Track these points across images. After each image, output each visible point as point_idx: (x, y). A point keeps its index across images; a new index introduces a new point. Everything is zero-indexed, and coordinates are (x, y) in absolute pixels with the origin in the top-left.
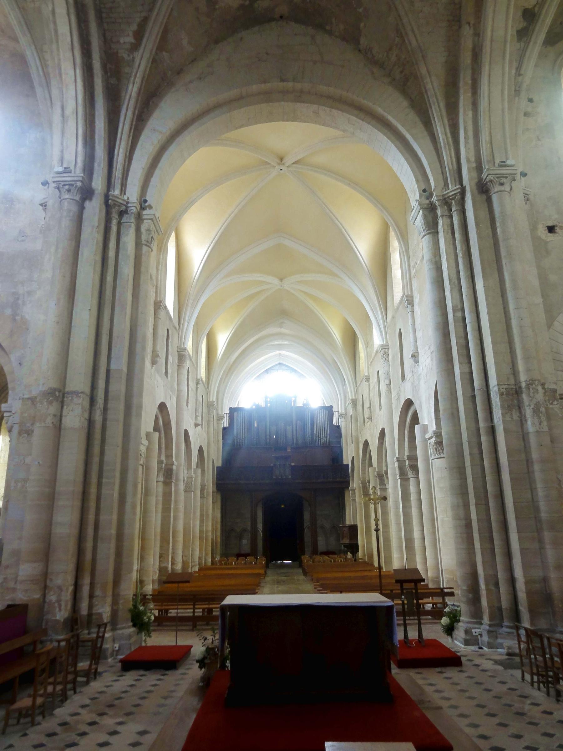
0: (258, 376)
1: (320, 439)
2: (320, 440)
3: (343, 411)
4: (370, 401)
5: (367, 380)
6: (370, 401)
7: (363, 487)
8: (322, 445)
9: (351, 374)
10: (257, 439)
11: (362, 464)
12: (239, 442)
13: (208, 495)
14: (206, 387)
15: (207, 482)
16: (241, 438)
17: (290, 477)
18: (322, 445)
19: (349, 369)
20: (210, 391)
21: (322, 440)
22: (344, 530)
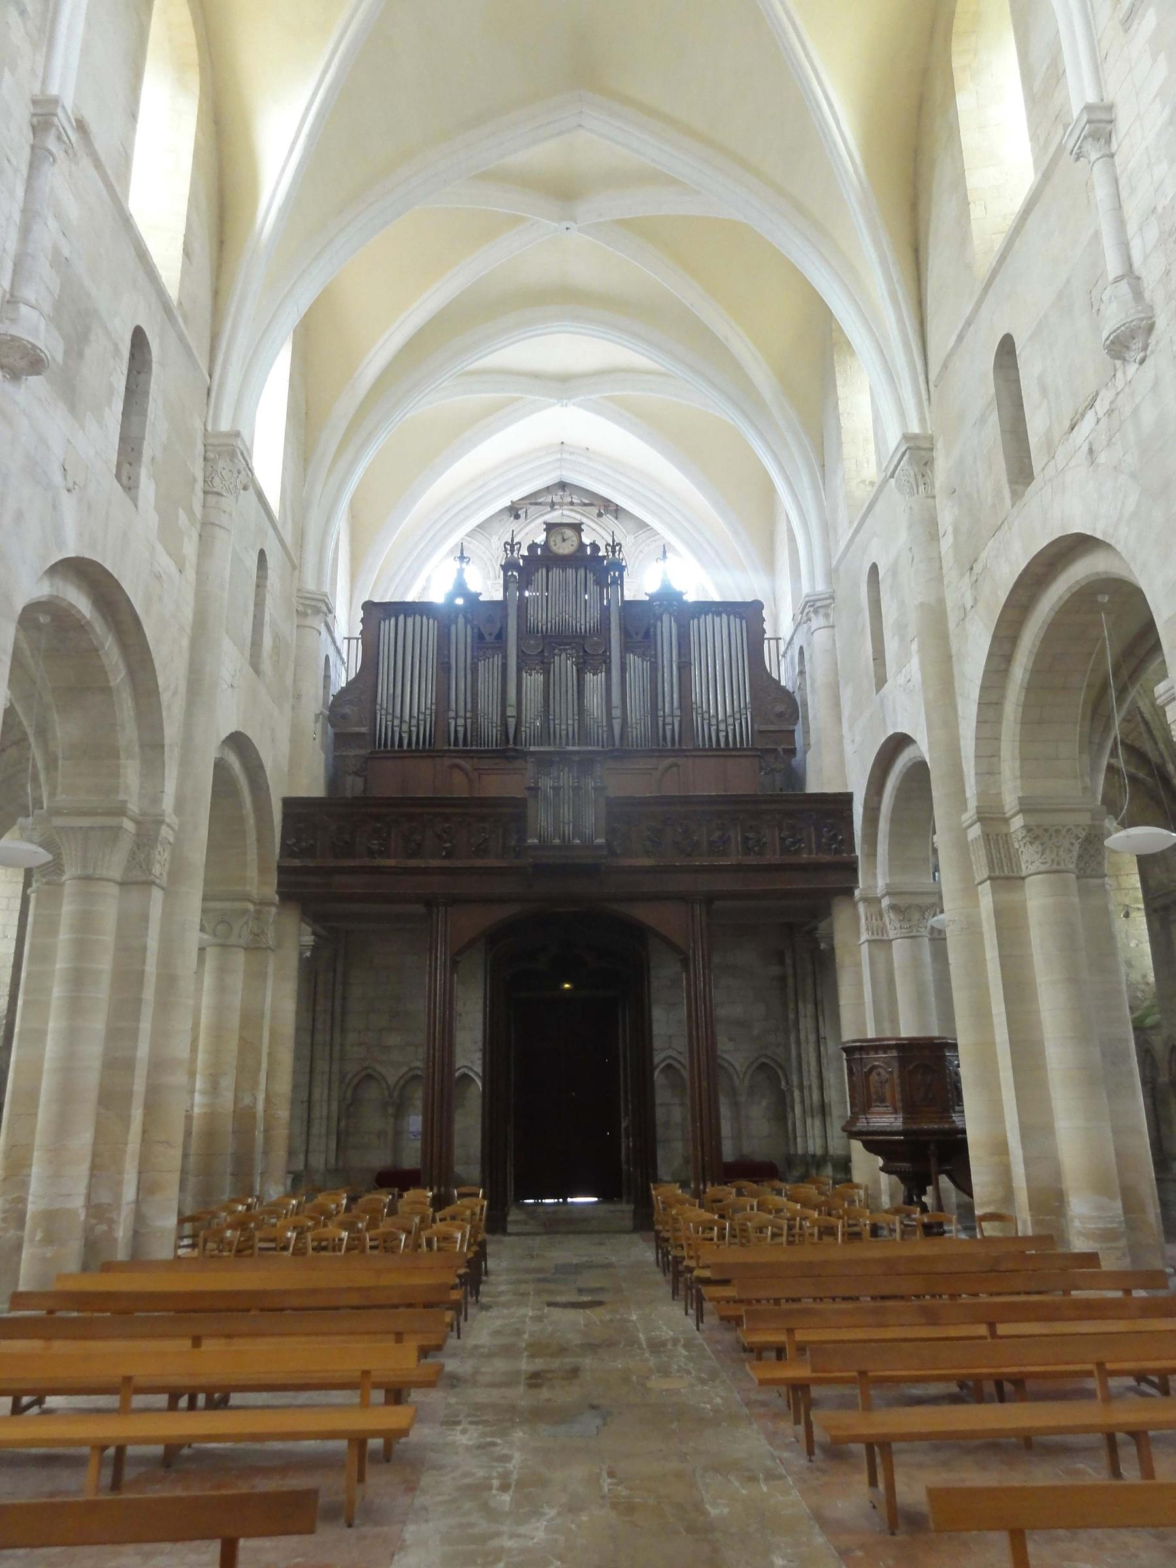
0: (481, 526)
1: (714, 721)
2: (713, 728)
3: (821, 587)
4: (1124, 246)
5: (1095, 136)
6: (1124, 246)
7: (986, 836)
8: (722, 745)
9: (900, 320)
10: (469, 721)
11: (981, 721)
12: (396, 729)
13: (177, 871)
14: (203, 364)
15: (179, 807)
16: (407, 718)
17: (600, 841)
18: (722, 745)
19: (893, 295)
20: (221, 385)
21: (722, 727)
22: (874, 1067)
